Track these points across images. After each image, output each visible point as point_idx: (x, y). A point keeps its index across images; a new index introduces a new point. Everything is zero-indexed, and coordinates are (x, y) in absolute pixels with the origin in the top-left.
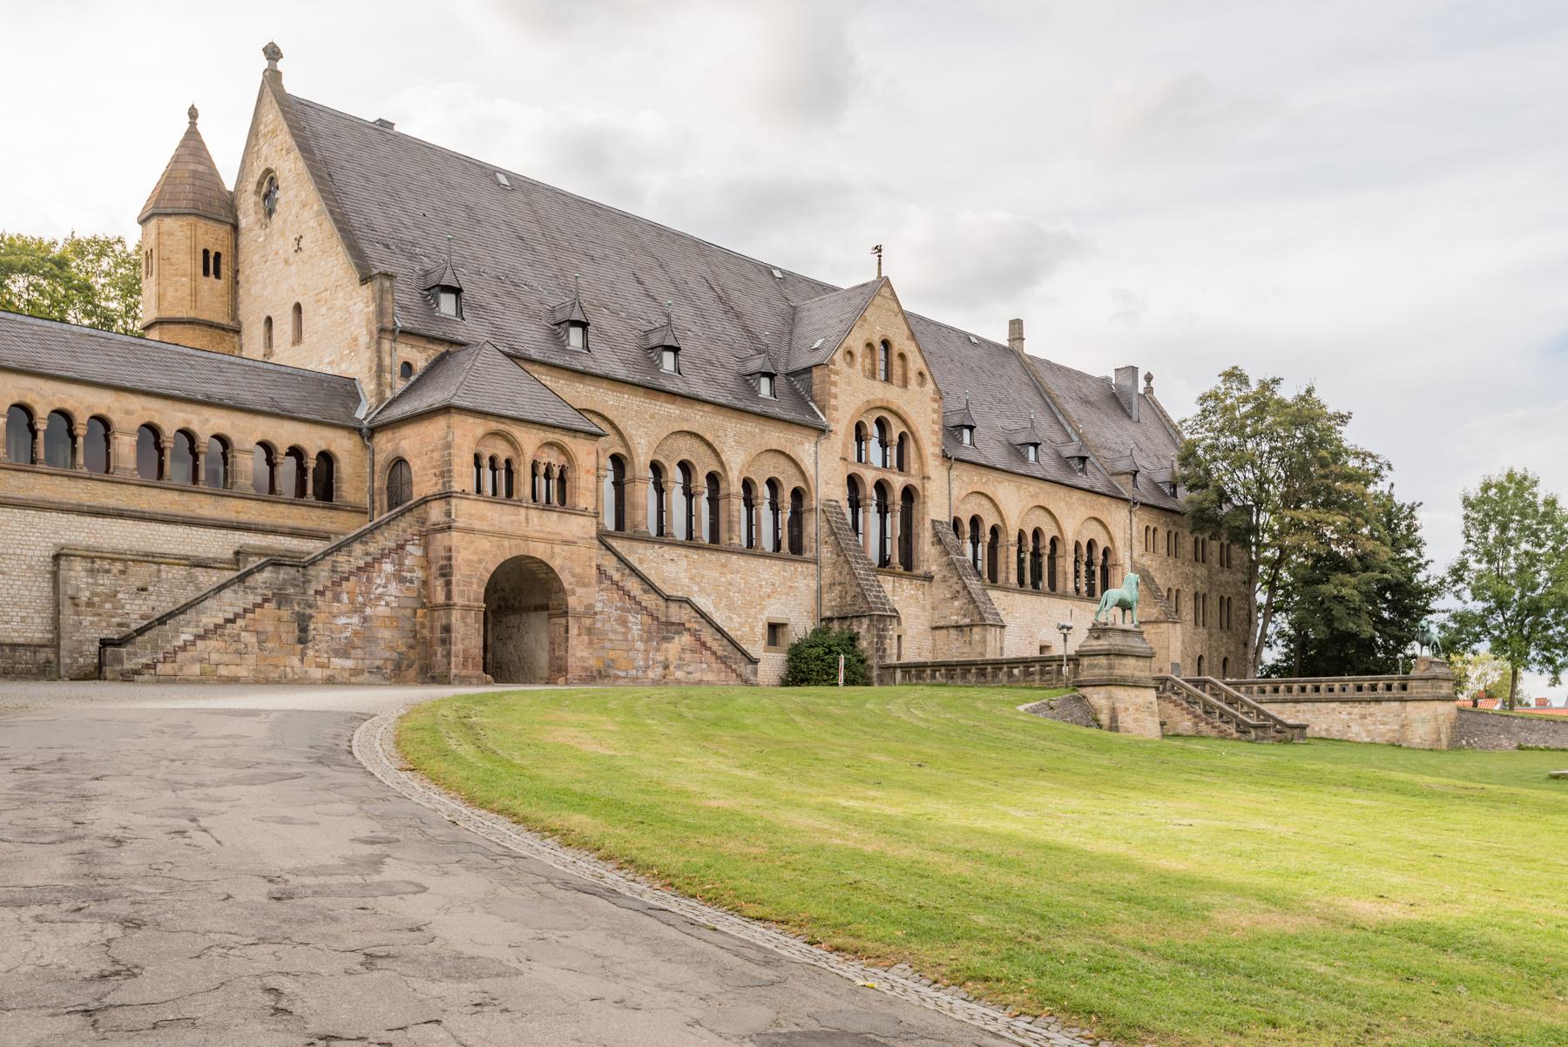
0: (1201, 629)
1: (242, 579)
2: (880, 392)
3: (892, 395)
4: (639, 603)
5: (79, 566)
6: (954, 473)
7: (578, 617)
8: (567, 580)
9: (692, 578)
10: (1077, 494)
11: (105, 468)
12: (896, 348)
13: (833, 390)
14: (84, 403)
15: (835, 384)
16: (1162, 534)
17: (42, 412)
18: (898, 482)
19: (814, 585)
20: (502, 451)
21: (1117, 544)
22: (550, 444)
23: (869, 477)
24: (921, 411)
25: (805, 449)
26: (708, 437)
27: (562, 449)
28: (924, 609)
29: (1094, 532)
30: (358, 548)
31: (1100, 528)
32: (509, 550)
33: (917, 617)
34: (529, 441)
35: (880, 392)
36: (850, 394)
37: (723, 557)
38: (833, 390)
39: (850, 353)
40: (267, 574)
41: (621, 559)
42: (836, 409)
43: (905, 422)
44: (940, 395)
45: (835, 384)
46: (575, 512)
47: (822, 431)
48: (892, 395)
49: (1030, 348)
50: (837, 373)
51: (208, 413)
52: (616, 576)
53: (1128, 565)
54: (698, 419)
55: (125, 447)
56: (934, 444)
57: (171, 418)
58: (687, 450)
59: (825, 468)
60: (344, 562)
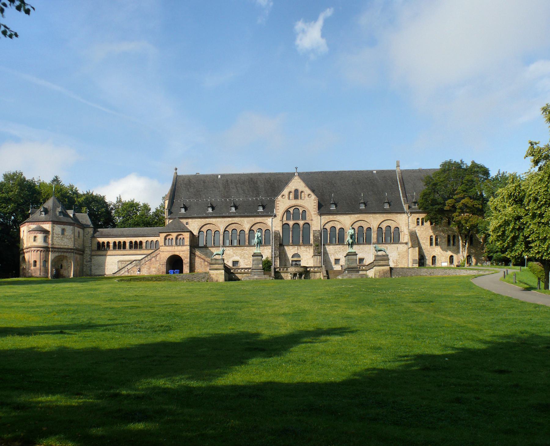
0: (451, 247)
2: (294, 202)
3: (298, 202)
5: (120, 263)
6: (322, 217)
7: (185, 264)
8: (183, 258)
9: (234, 253)
12: (300, 190)
14: (122, 240)
18: (301, 223)
23: (291, 223)
25: (268, 221)
30: (149, 256)
35: (294, 202)
37: (242, 248)
46: (183, 245)
55: (128, 245)
57: (134, 240)
58: (233, 227)
60: (146, 259)
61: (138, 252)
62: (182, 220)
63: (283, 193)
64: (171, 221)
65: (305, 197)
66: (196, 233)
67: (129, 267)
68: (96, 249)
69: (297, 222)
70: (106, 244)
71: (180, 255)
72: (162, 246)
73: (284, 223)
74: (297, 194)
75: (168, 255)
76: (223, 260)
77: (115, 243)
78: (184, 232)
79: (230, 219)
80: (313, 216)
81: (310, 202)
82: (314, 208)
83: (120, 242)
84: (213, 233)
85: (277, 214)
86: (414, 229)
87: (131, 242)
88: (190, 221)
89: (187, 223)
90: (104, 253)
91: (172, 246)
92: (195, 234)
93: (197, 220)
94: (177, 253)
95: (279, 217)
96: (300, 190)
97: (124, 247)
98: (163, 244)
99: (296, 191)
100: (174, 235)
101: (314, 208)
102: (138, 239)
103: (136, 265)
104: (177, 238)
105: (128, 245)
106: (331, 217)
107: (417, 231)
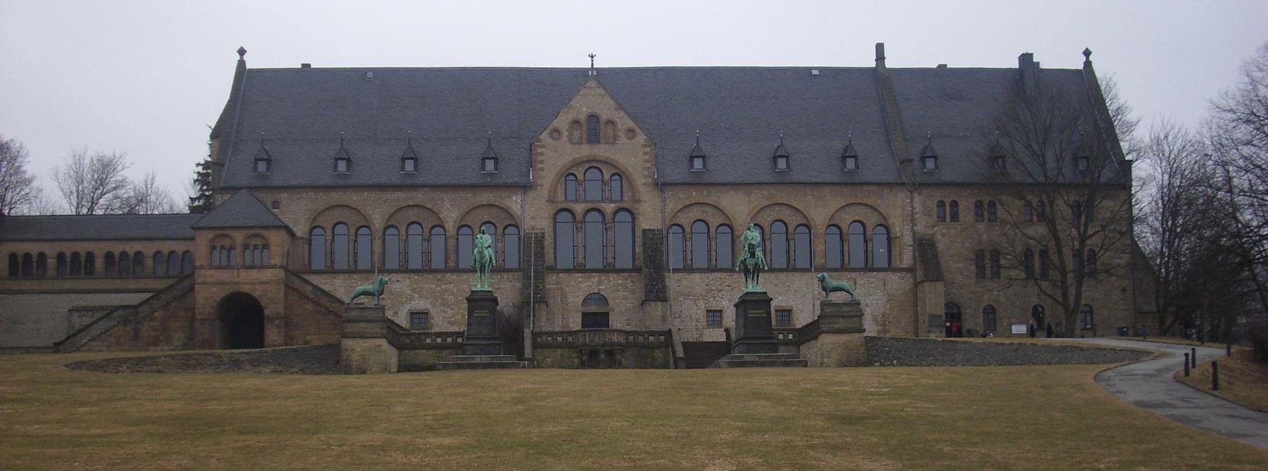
1: (108, 315)
2: (586, 151)
3: (601, 151)
4: (327, 309)
6: (669, 194)
9: (413, 290)
10: (827, 191)
11: (90, 272)
12: (604, 118)
13: (540, 158)
15: (542, 154)
16: (966, 204)
17: (68, 254)
19: (519, 285)
20: (227, 242)
21: (890, 221)
22: (256, 235)
24: (631, 154)
25: (515, 203)
26: (428, 206)
27: (263, 237)
28: (633, 292)
29: (859, 214)
31: (869, 210)
32: (226, 290)
33: (626, 298)
34: (239, 237)
35: (586, 151)
36: (556, 155)
38: (540, 158)
39: (556, 131)
40: (120, 312)
41: (315, 287)
42: (542, 169)
43: (616, 167)
44: (652, 141)
45: (542, 154)
47: (526, 187)
48: (601, 151)
49: (890, 63)
50: (543, 147)
51: (132, 243)
52: (311, 296)
53: (908, 238)
54: (419, 197)
55: (99, 263)
56: (645, 176)
57: (117, 249)
58: (412, 215)
59: (533, 211)
61: (131, 284)
62: (261, 195)
63: (555, 123)
64: (227, 197)
65: (616, 138)
66: (300, 230)
67: (103, 325)
68: (6, 273)
69: (596, 206)
70: (35, 259)
71: (257, 294)
72: (202, 267)
73: (561, 206)
74: (593, 129)
75: (218, 293)
76: (383, 309)
77: (61, 256)
78: (267, 228)
79: (401, 195)
80: (642, 189)
81: (631, 154)
82: (644, 169)
83: (75, 255)
84: (353, 231)
85: (540, 181)
86: (929, 231)
87: (109, 256)
88: (284, 196)
89: (276, 204)
90: (27, 284)
91: (228, 267)
92: (299, 234)
93: (304, 195)
94: (246, 289)
95: (544, 192)
96: (604, 118)
97: (90, 272)
98: (204, 262)
99: (593, 118)
100: (239, 237)
101: (644, 169)
102: (132, 248)
103: (126, 322)
104: (246, 247)
105: (99, 263)
106: (695, 195)
107: (939, 237)
